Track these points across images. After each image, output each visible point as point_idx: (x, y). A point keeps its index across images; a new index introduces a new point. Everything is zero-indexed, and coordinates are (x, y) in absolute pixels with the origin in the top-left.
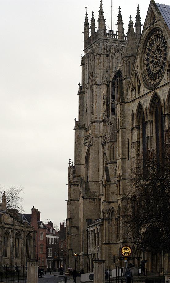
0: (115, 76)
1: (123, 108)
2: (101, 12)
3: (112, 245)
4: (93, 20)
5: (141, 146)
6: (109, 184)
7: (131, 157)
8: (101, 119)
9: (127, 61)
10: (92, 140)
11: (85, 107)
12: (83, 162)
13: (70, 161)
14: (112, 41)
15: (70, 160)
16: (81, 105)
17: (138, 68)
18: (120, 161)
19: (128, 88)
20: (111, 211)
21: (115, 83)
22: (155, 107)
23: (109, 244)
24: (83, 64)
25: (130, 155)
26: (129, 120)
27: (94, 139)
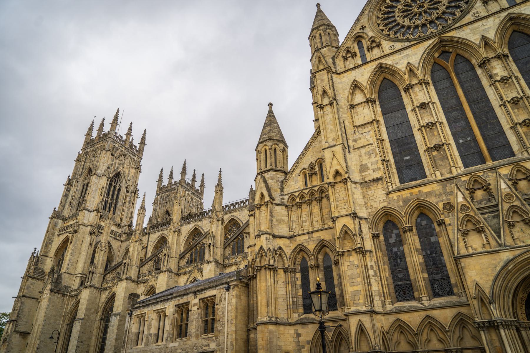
0: (114, 176)
1: (332, 77)
2: (116, 118)
3: (282, 328)
4: (102, 124)
5: (383, 129)
6: (272, 203)
7: (355, 147)
8: (93, 209)
9: (326, 29)
10: (79, 228)
11: (70, 198)
12: (52, 253)
13: (35, 250)
14: (120, 145)
15: (36, 249)
16: (66, 196)
17: (365, 29)
18: (338, 149)
19: (334, 57)
20: (276, 254)
21: (112, 181)
22: (430, 63)
23: (276, 323)
24: (78, 160)
25: (351, 143)
26: (342, 96)
27: (81, 226)
